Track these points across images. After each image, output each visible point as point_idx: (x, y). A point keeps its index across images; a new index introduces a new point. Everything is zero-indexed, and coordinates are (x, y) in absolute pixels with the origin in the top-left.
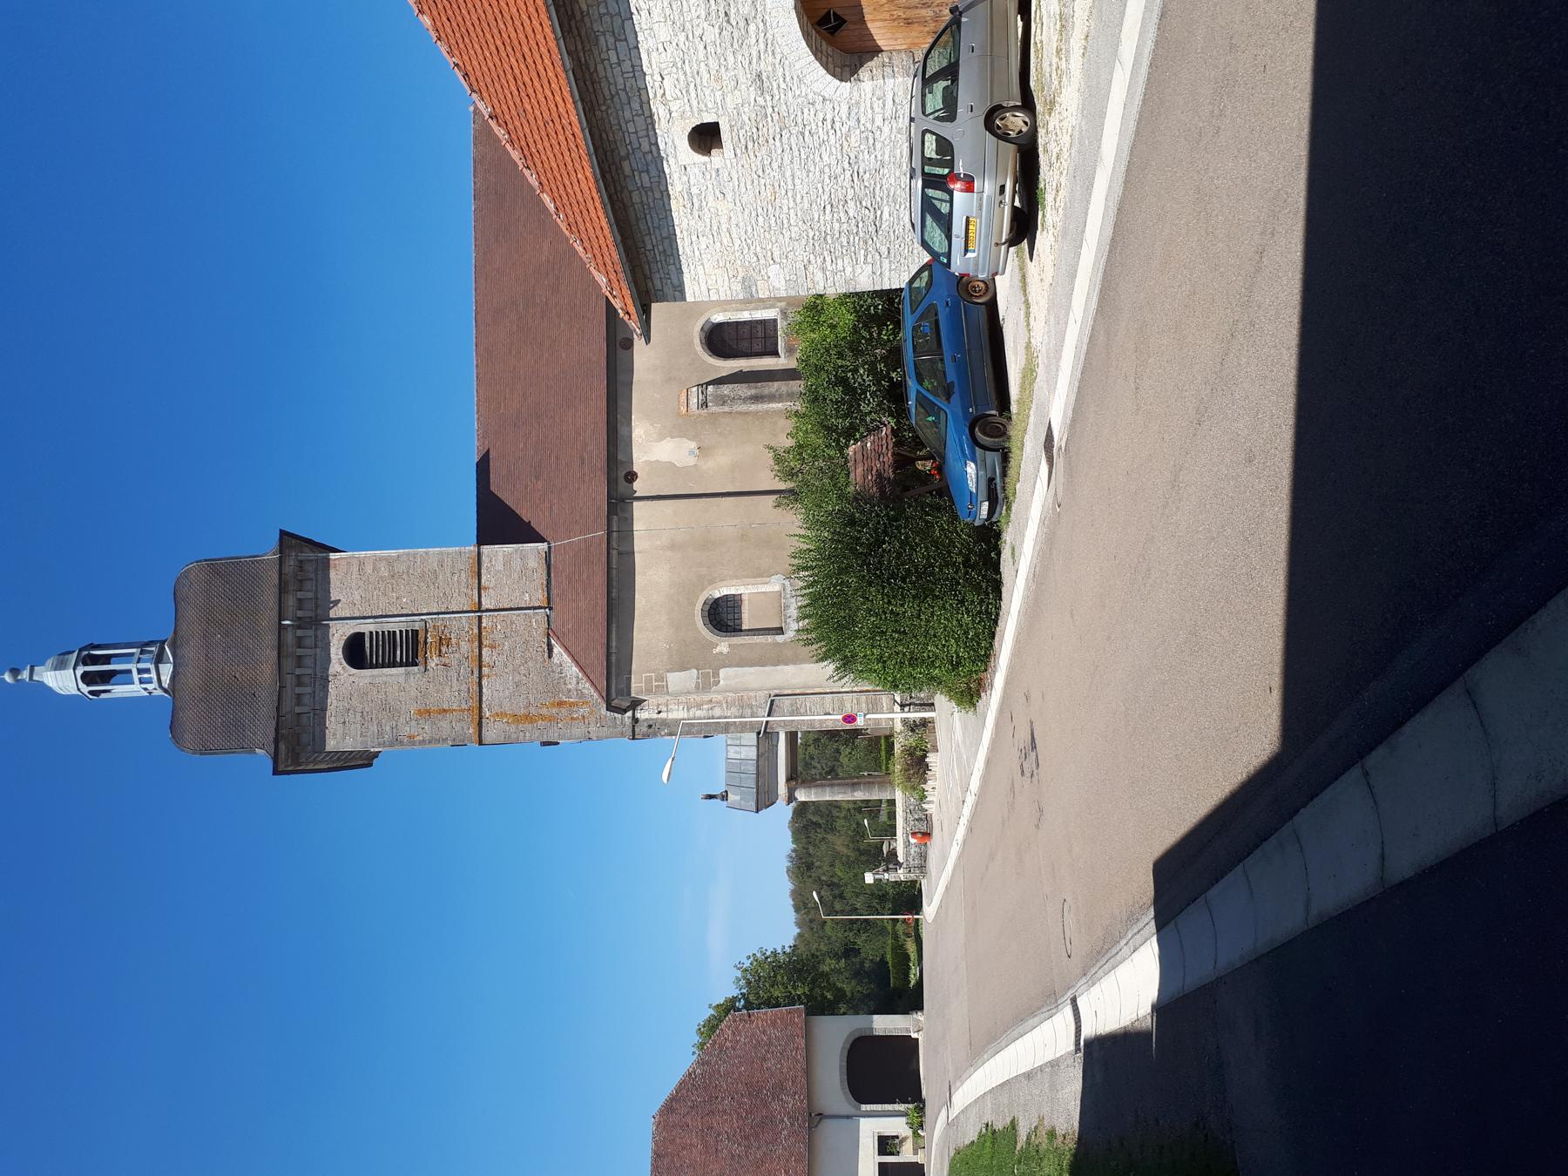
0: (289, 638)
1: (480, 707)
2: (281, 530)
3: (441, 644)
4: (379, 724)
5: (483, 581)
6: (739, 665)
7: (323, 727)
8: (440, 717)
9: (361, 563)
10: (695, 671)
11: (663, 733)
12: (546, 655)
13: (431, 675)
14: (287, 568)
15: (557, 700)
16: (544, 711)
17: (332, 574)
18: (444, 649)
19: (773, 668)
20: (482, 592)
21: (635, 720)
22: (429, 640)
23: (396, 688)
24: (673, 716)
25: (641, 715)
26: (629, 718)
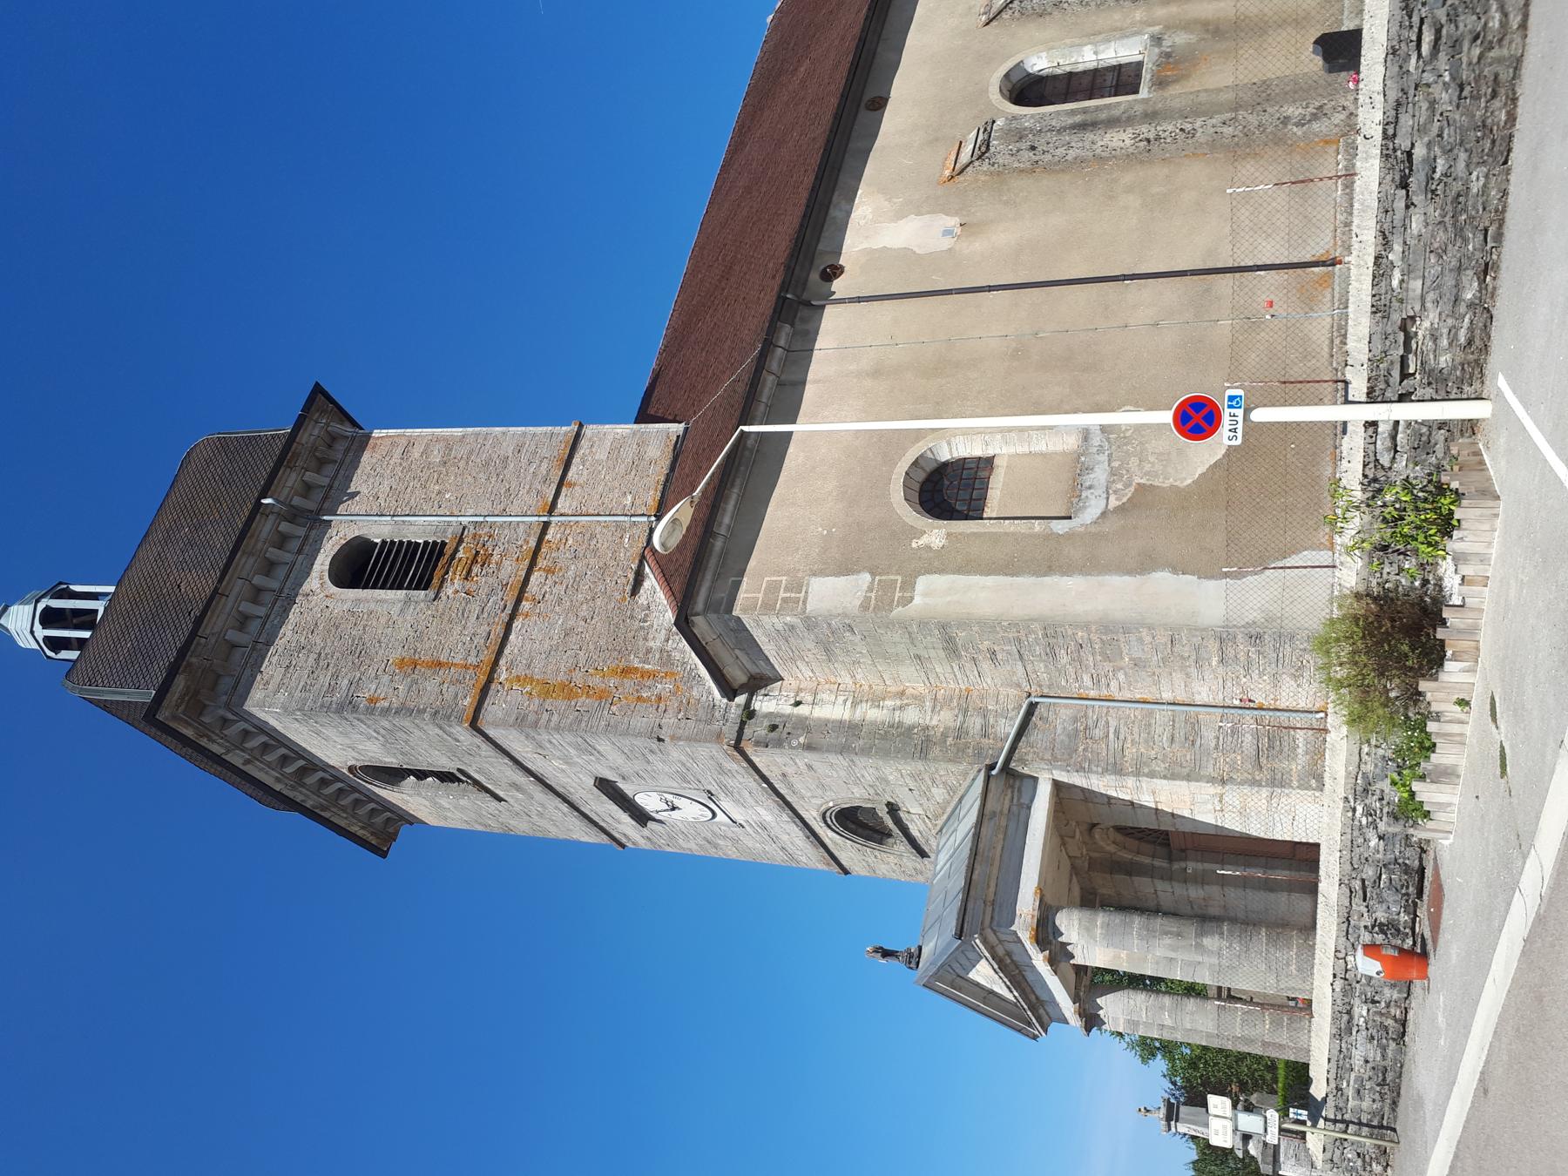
0: (265, 528)
1: (496, 663)
2: (317, 384)
3: (474, 561)
4: (335, 676)
5: (570, 474)
6: (959, 570)
7: (257, 667)
8: (429, 672)
9: (411, 443)
10: (867, 577)
11: (794, 743)
12: (628, 588)
13: (441, 607)
14: (306, 435)
15: (622, 665)
16: (595, 681)
17: (366, 457)
18: (476, 569)
19: (1033, 579)
20: (564, 489)
21: (749, 713)
22: (460, 554)
23: (383, 620)
24: (820, 713)
25: (763, 704)
26: (738, 706)
